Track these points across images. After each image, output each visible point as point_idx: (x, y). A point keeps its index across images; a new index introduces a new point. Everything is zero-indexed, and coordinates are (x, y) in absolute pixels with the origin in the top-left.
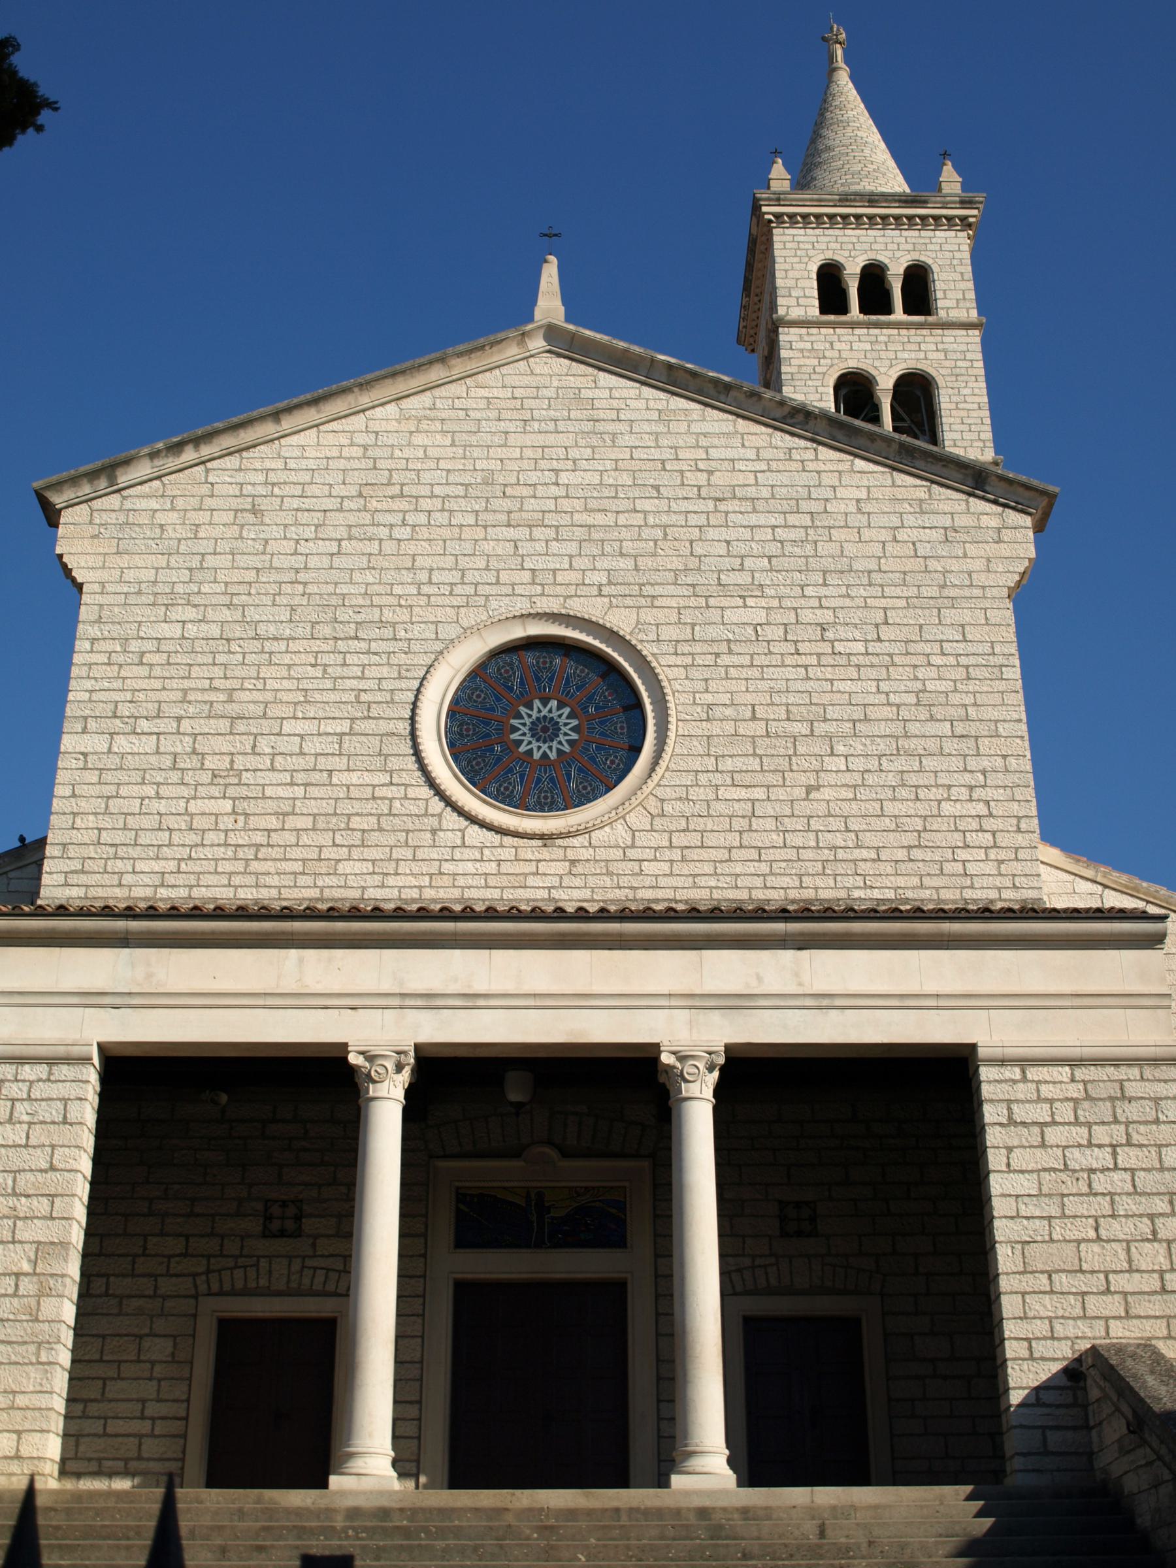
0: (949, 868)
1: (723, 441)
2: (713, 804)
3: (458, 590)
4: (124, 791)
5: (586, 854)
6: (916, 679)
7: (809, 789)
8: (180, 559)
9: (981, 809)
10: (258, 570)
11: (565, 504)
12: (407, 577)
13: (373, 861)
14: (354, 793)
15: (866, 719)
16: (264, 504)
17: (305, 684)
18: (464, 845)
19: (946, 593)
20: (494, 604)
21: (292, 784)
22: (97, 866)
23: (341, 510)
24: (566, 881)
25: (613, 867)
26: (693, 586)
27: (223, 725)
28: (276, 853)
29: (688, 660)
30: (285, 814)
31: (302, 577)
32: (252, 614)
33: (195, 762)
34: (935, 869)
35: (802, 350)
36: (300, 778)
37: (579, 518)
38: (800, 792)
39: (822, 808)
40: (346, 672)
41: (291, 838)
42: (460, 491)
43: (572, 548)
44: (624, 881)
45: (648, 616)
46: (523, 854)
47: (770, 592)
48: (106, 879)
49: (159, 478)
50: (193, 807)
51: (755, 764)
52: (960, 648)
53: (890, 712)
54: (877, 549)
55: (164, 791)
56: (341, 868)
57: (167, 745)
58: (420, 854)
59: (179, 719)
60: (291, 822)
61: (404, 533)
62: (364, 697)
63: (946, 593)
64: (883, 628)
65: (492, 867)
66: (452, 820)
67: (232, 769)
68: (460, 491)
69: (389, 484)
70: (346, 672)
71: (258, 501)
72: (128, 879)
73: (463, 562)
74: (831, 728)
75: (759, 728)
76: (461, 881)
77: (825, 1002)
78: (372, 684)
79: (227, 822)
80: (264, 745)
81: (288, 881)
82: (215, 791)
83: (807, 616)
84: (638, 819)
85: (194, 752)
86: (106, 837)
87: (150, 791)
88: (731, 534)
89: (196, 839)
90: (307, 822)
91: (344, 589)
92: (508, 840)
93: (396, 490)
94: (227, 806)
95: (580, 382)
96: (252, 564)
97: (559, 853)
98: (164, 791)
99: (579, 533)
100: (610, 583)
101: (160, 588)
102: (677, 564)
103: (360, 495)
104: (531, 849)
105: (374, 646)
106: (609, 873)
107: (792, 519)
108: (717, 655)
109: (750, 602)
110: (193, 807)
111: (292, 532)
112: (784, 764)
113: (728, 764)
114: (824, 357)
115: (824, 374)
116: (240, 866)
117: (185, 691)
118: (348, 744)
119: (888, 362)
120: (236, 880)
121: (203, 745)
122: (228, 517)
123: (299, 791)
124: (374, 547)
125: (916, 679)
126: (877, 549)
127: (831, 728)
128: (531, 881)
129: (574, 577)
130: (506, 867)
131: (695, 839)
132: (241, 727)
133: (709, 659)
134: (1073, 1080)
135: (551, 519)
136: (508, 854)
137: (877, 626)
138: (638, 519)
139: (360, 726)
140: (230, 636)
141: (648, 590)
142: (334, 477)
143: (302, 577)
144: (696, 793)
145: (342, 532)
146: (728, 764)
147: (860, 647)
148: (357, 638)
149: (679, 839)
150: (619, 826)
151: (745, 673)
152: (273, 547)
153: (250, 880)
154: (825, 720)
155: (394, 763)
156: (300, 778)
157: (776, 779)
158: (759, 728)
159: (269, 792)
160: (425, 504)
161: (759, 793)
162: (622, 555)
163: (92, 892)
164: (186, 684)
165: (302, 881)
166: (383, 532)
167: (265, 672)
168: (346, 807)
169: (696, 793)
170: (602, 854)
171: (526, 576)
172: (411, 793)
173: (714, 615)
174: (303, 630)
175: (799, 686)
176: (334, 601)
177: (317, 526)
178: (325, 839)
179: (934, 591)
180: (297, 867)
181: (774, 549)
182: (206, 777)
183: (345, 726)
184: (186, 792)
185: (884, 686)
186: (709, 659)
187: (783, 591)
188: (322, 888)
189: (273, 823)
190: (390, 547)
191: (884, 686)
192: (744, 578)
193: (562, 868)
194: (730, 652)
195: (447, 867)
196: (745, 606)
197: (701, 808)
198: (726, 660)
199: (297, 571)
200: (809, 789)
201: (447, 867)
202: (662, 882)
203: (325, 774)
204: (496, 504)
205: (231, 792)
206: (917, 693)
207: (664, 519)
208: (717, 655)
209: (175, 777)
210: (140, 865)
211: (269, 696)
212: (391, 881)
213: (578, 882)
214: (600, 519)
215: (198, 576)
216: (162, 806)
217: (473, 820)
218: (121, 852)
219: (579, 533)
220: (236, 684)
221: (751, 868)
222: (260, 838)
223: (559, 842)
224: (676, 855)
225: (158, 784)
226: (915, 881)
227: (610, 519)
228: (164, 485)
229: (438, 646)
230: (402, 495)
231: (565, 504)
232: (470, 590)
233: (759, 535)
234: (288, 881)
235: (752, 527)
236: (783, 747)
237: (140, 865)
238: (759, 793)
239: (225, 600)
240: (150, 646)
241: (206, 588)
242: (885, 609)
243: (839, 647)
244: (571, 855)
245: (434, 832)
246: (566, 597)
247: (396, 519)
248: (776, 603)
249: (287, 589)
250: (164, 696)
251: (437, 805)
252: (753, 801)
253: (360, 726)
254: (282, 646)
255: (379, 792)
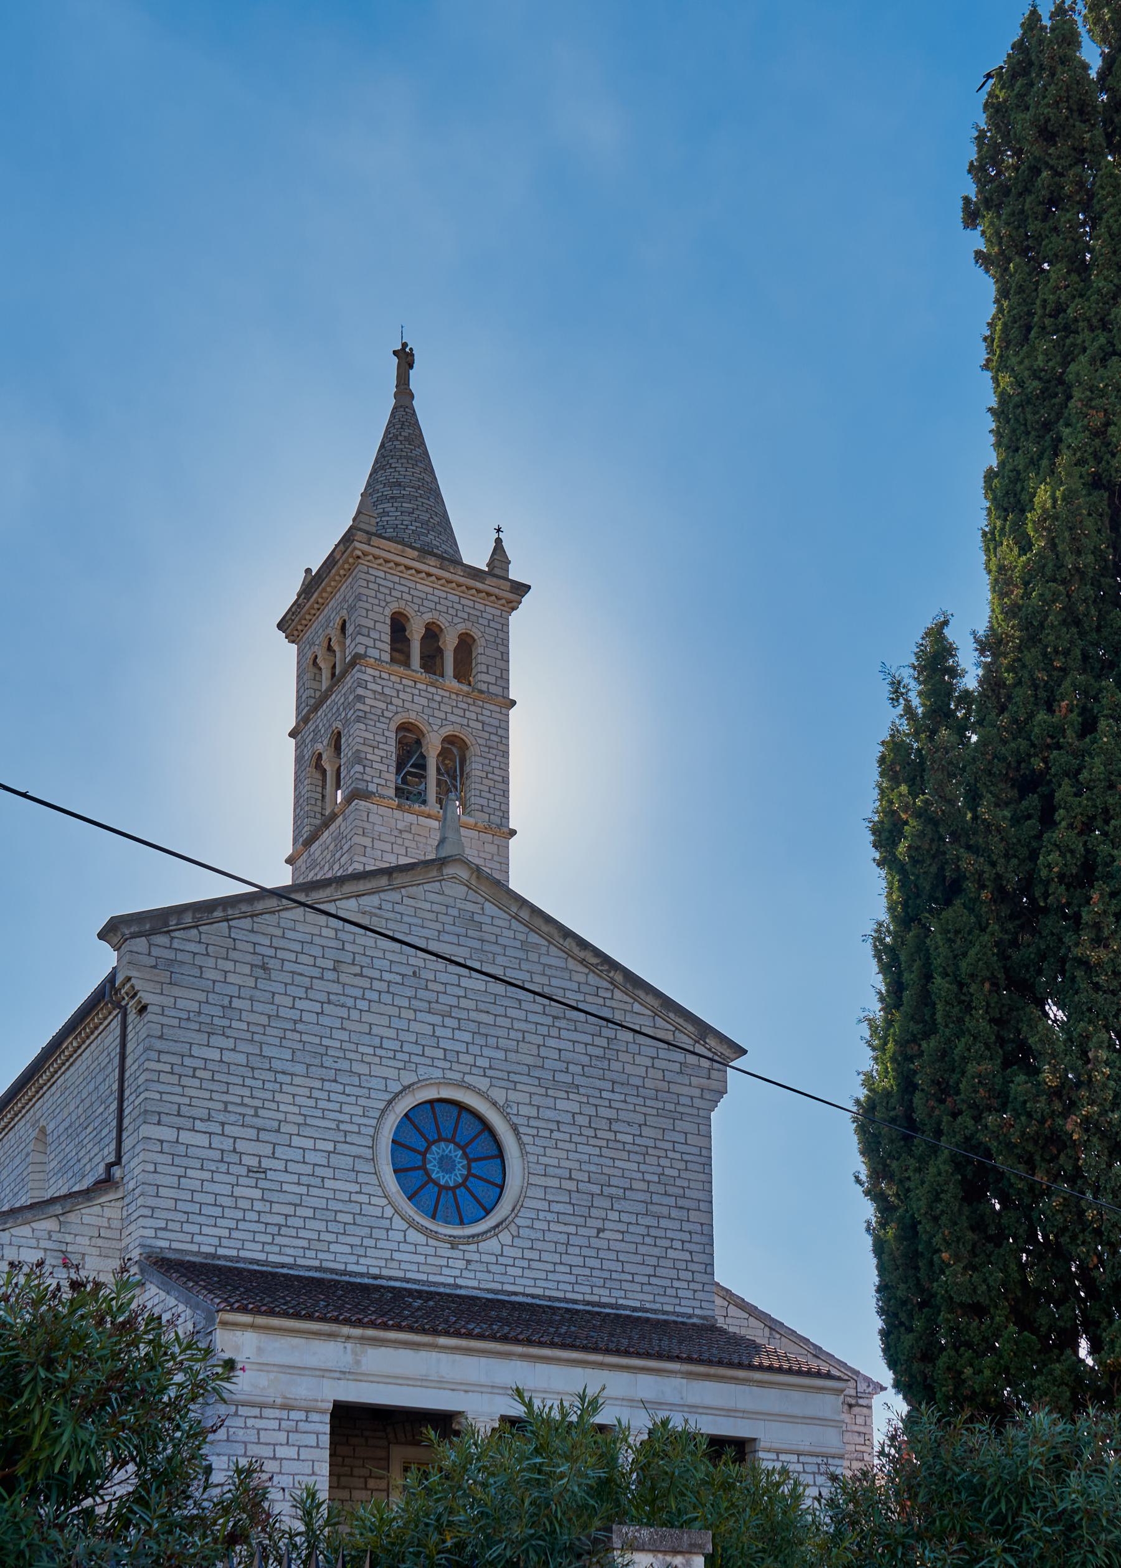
0: (669, 1291)
1: (558, 973)
2: (547, 1233)
3: (399, 1056)
4: (190, 1173)
5: (476, 1257)
6: (659, 1165)
7: (600, 1231)
8: (216, 997)
9: (687, 1257)
10: (269, 1016)
11: (464, 1003)
12: (366, 1039)
13: (352, 1246)
14: (338, 1196)
15: (631, 1189)
16: (272, 964)
17: (304, 1111)
18: (405, 1241)
19: (680, 1109)
20: (421, 1070)
21: (299, 1184)
22: (177, 1226)
23: (322, 978)
24: (465, 1274)
25: (491, 1267)
26: (539, 1079)
27: (252, 1133)
28: (293, 1232)
29: (534, 1132)
30: (295, 1205)
31: (299, 1027)
32: (267, 1051)
33: (234, 1158)
34: (661, 1291)
35: (375, 692)
36: (304, 1180)
37: (473, 1015)
38: (594, 1232)
39: (605, 1244)
40: (331, 1106)
41: (299, 1223)
42: (399, 979)
43: (467, 1037)
44: (497, 1278)
45: (513, 1096)
46: (440, 1252)
47: (582, 1090)
48: (181, 1236)
49: (197, 927)
50: (238, 1191)
51: (569, 1209)
52: (684, 1148)
53: (644, 1186)
54: (642, 1071)
55: (217, 1177)
56: (333, 1247)
57: (216, 1142)
58: (380, 1244)
59: (223, 1124)
60: (300, 1211)
61: (363, 1005)
62: (342, 1127)
63: (680, 1109)
64: (643, 1127)
65: (422, 1259)
66: (398, 1223)
67: (260, 1167)
68: (399, 979)
69: (353, 964)
70: (331, 1106)
71: (266, 960)
72: (197, 1239)
73: (403, 1036)
74: (613, 1191)
75: (571, 1185)
76: (404, 1266)
77: (694, 1410)
78: (347, 1118)
79: (258, 1206)
80: (279, 1152)
81: (300, 1252)
82: (252, 1182)
83: (604, 1112)
84: (505, 1237)
85: (234, 1151)
86: (181, 1206)
87: (207, 1175)
88: (563, 1045)
89: (239, 1215)
90: (309, 1213)
91: (325, 1042)
92: (431, 1242)
93: (357, 970)
94: (257, 1194)
95: (470, 907)
96: (267, 1011)
97: (460, 1254)
98: (217, 1177)
99: (473, 1027)
100: (490, 1068)
101: (203, 1018)
102: (530, 1060)
103: (334, 969)
104: (445, 1250)
105: (348, 1090)
106: (489, 1272)
107: (598, 1041)
108: (552, 1131)
109: (571, 1096)
110: (238, 1191)
111: (291, 990)
112: (585, 1211)
113: (556, 1207)
114: (391, 703)
115: (390, 719)
116: (269, 1239)
117: (226, 1103)
118: (335, 1160)
119: (439, 722)
120: (267, 1248)
121: (241, 1146)
122: (247, 970)
123: (304, 1190)
124: (343, 1013)
125: (659, 1165)
126: (642, 1071)
127: (613, 1191)
128: (445, 1271)
129: (470, 1059)
130: (430, 1260)
131: (534, 1255)
132: (263, 1136)
133: (547, 1134)
134: (798, 1462)
135: (455, 1013)
136: (431, 1251)
137: (640, 1125)
138: (507, 1023)
139: (341, 1147)
140: (255, 1066)
141: (513, 1077)
142: (317, 952)
143: (299, 1027)
144: (538, 1225)
145: (323, 997)
146: (556, 1207)
147: (629, 1139)
148: (335, 1081)
149: (528, 1254)
150: (494, 1240)
151: (567, 1146)
152: (278, 999)
153: (276, 1249)
154: (609, 1186)
155: (362, 1178)
156: (304, 1180)
157: (581, 1221)
158: (571, 1185)
159: (285, 1187)
160: (377, 985)
161: (572, 1229)
162: (497, 1048)
163: (175, 1245)
164: (225, 1098)
165: (309, 1254)
166: (350, 1002)
167: (278, 1097)
168: (333, 1205)
169: (538, 1225)
170: (485, 1258)
171: (440, 1054)
172: (374, 1200)
173: (550, 1102)
174: (300, 1069)
175: (595, 1160)
176: (322, 1050)
177: (307, 989)
178: (321, 1226)
179: (671, 1107)
180: (305, 1243)
181: (585, 1060)
182: (243, 1171)
183: (330, 1147)
184: (233, 1180)
185: (643, 1168)
186: (547, 1134)
187: (591, 1092)
188: (321, 1260)
189: (289, 1210)
190: (355, 1014)
191: (643, 1168)
192: (568, 1079)
193: (461, 1264)
194: (559, 1130)
195: (396, 1255)
196: (568, 1099)
197: (539, 1235)
198: (556, 1135)
199: (295, 1022)
200: (600, 1231)
201: (396, 1255)
202: (518, 1281)
203: (320, 1180)
204: (421, 994)
205: (261, 1184)
206: (659, 1175)
207: (523, 1026)
208: (552, 1131)
209: (223, 1168)
210: (205, 1230)
211: (281, 1116)
212: (362, 1261)
213: (472, 1275)
214: (484, 1018)
215: (229, 1013)
216: (216, 1188)
217: (412, 1224)
218: (192, 1218)
219: (473, 1027)
220: (259, 1103)
221: (567, 1278)
222: (281, 1220)
223: (461, 1247)
224: (525, 1264)
225: (213, 1172)
226: (651, 1298)
227: (489, 1019)
228: (200, 933)
229: (388, 1097)
230: (361, 975)
231: (464, 1003)
232: (406, 1057)
233: (580, 1048)
234: (300, 1252)
235: (574, 1042)
236: (585, 1200)
237: (205, 1230)
238: (572, 1229)
239: (248, 1036)
240: (200, 1063)
241: (235, 1024)
242: (645, 1115)
243: (619, 1137)
244: (468, 1256)
245: (388, 1230)
246: (464, 1074)
247: (358, 993)
248: (585, 1100)
249: (289, 1034)
250: (210, 1104)
251: (389, 1212)
252: (568, 1234)
253: (341, 1147)
254: (288, 1079)
255: (354, 1197)
